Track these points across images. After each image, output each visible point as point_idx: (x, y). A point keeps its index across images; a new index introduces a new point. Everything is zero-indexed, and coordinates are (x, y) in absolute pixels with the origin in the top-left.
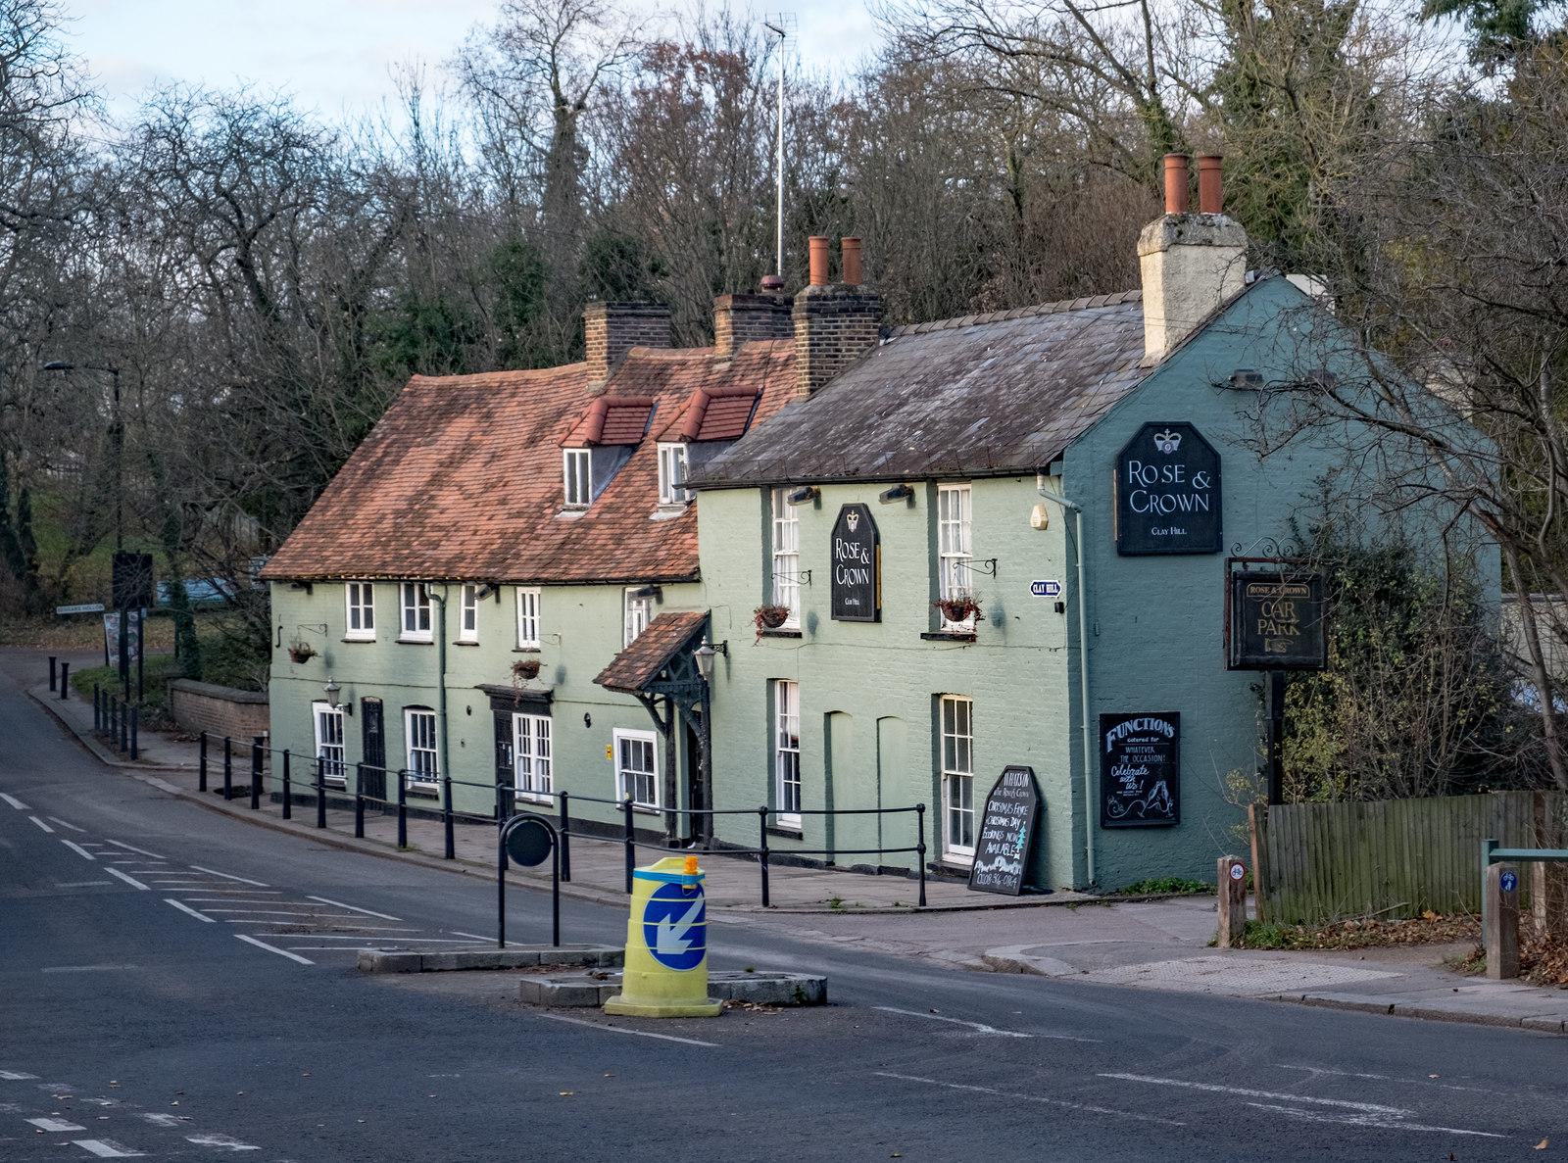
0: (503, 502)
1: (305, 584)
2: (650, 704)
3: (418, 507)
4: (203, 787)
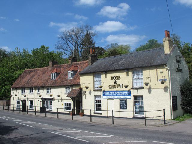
0: (41, 79)
1: (16, 89)
2: (72, 99)
3: (29, 80)
4: (4, 109)
